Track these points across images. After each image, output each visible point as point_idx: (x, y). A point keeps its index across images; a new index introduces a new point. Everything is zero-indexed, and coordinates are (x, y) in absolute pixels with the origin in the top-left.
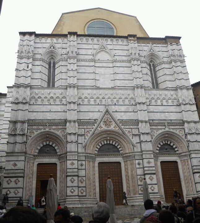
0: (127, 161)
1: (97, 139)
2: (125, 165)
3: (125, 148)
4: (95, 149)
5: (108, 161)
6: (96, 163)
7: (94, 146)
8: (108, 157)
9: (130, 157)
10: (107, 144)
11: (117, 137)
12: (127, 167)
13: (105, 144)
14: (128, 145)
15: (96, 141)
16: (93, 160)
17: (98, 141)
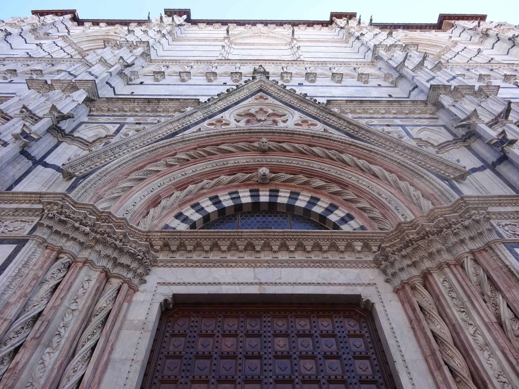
0: (426, 276)
1: (190, 170)
2: (417, 316)
3: (383, 206)
4: (161, 218)
5: (254, 290)
6: (138, 297)
7: (155, 202)
8: (250, 264)
9: (445, 239)
10: (256, 205)
11: (316, 165)
12: (441, 328)
13: (239, 208)
14: (402, 184)
15: (178, 175)
16: (116, 263)
17: (194, 181)
